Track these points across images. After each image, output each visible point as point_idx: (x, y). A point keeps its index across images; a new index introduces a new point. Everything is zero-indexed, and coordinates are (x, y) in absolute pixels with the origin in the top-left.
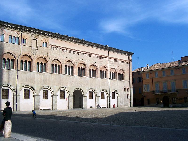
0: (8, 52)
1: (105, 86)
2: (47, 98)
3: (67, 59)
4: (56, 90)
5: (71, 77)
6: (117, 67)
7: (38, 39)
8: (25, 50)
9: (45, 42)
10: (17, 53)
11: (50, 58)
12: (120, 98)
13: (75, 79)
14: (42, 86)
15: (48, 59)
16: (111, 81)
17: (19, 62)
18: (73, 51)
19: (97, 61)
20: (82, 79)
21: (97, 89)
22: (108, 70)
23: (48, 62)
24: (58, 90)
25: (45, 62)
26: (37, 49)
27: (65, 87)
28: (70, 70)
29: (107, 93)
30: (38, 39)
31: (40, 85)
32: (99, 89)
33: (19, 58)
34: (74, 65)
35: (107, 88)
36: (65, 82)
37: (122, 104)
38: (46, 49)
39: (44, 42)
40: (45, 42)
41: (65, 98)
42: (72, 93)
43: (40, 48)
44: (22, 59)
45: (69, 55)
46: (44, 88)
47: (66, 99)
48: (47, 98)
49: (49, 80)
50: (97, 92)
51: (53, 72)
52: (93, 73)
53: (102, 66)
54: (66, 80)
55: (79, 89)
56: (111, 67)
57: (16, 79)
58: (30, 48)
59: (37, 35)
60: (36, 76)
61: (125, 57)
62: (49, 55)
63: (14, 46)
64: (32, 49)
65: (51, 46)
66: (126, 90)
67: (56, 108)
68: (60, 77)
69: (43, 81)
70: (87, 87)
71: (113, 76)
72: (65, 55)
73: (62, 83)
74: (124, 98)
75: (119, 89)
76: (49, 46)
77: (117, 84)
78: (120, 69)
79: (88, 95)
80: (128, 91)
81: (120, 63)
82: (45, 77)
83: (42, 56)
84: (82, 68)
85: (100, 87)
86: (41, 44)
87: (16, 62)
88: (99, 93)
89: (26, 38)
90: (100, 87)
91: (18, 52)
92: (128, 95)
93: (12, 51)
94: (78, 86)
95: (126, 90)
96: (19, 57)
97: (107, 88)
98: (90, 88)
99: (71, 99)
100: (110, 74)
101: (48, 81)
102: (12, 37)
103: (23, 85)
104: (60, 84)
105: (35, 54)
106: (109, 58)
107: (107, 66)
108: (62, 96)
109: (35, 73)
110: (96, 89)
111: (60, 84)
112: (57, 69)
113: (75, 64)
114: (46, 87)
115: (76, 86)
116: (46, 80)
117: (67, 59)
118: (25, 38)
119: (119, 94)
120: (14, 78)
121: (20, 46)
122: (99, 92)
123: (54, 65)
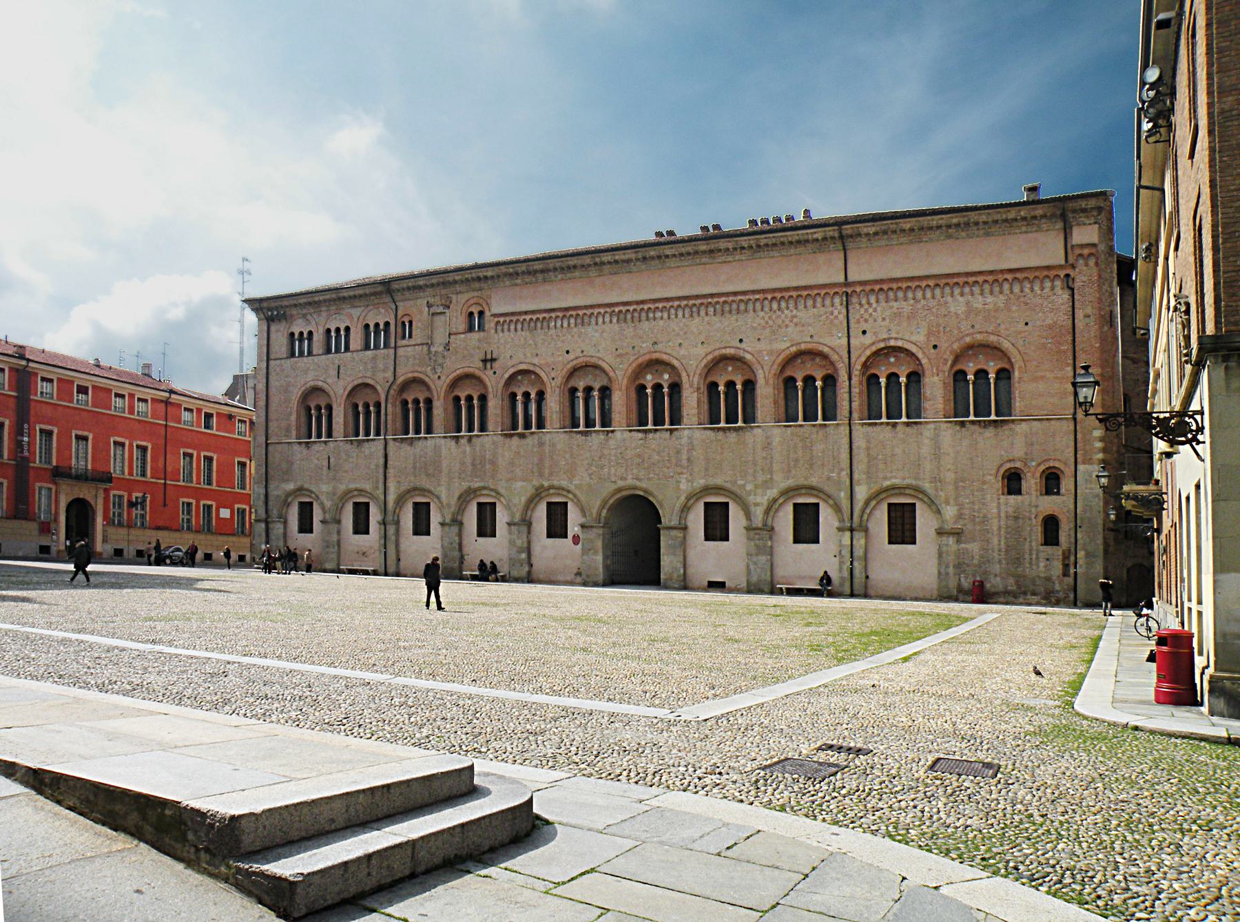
0: (360, 381)
1: (811, 465)
3: (571, 356)
4: (523, 499)
6: (929, 334)
8: (410, 361)
9: (475, 310)
12: (958, 542)
13: (612, 442)
14: (465, 485)
15: (489, 378)
19: (754, 328)
20: (659, 439)
21: (756, 487)
23: (490, 390)
27: (564, 483)
28: (588, 403)
29: (837, 508)
31: (459, 487)
32: (767, 484)
35: (828, 476)
38: (479, 340)
40: (475, 310)
47: (576, 540)
49: (493, 463)
50: (756, 505)
52: (730, 402)
54: (567, 456)
55: (641, 493)
56: (864, 345)
57: (381, 470)
59: (443, 292)
60: (444, 451)
61: (1045, 248)
62: (493, 360)
63: (374, 358)
64: (429, 352)
66: (1031, 483)
68: (541, 444)
69: (470, 468)
70: (683, 481)
73: (547, 471)
74: (997, 542)
75: (950, 476)
76: (490, 324)
77: (926, 450)
81: (957, 304)
82: (478, 449)
83: (467, 370)
85: (778, 477)
95: (1031, 483)
96: (392, 392)
97: (829, 478)
98: (700, 482)
99: (596, 539)
101: (488, 466)
103: (403, 488)
104: (541, 475)
105: (439, 370)
106: (848, 291)
107: (833, 342)
108: (557, 528)
109: (443, 441)
110: (749, 487)
111: (541, 475)
114: (484, 488)
115: (621, 479)
117: (571, 356)
118: (406, 320)
119: (950, 512)
121: (392, 351)
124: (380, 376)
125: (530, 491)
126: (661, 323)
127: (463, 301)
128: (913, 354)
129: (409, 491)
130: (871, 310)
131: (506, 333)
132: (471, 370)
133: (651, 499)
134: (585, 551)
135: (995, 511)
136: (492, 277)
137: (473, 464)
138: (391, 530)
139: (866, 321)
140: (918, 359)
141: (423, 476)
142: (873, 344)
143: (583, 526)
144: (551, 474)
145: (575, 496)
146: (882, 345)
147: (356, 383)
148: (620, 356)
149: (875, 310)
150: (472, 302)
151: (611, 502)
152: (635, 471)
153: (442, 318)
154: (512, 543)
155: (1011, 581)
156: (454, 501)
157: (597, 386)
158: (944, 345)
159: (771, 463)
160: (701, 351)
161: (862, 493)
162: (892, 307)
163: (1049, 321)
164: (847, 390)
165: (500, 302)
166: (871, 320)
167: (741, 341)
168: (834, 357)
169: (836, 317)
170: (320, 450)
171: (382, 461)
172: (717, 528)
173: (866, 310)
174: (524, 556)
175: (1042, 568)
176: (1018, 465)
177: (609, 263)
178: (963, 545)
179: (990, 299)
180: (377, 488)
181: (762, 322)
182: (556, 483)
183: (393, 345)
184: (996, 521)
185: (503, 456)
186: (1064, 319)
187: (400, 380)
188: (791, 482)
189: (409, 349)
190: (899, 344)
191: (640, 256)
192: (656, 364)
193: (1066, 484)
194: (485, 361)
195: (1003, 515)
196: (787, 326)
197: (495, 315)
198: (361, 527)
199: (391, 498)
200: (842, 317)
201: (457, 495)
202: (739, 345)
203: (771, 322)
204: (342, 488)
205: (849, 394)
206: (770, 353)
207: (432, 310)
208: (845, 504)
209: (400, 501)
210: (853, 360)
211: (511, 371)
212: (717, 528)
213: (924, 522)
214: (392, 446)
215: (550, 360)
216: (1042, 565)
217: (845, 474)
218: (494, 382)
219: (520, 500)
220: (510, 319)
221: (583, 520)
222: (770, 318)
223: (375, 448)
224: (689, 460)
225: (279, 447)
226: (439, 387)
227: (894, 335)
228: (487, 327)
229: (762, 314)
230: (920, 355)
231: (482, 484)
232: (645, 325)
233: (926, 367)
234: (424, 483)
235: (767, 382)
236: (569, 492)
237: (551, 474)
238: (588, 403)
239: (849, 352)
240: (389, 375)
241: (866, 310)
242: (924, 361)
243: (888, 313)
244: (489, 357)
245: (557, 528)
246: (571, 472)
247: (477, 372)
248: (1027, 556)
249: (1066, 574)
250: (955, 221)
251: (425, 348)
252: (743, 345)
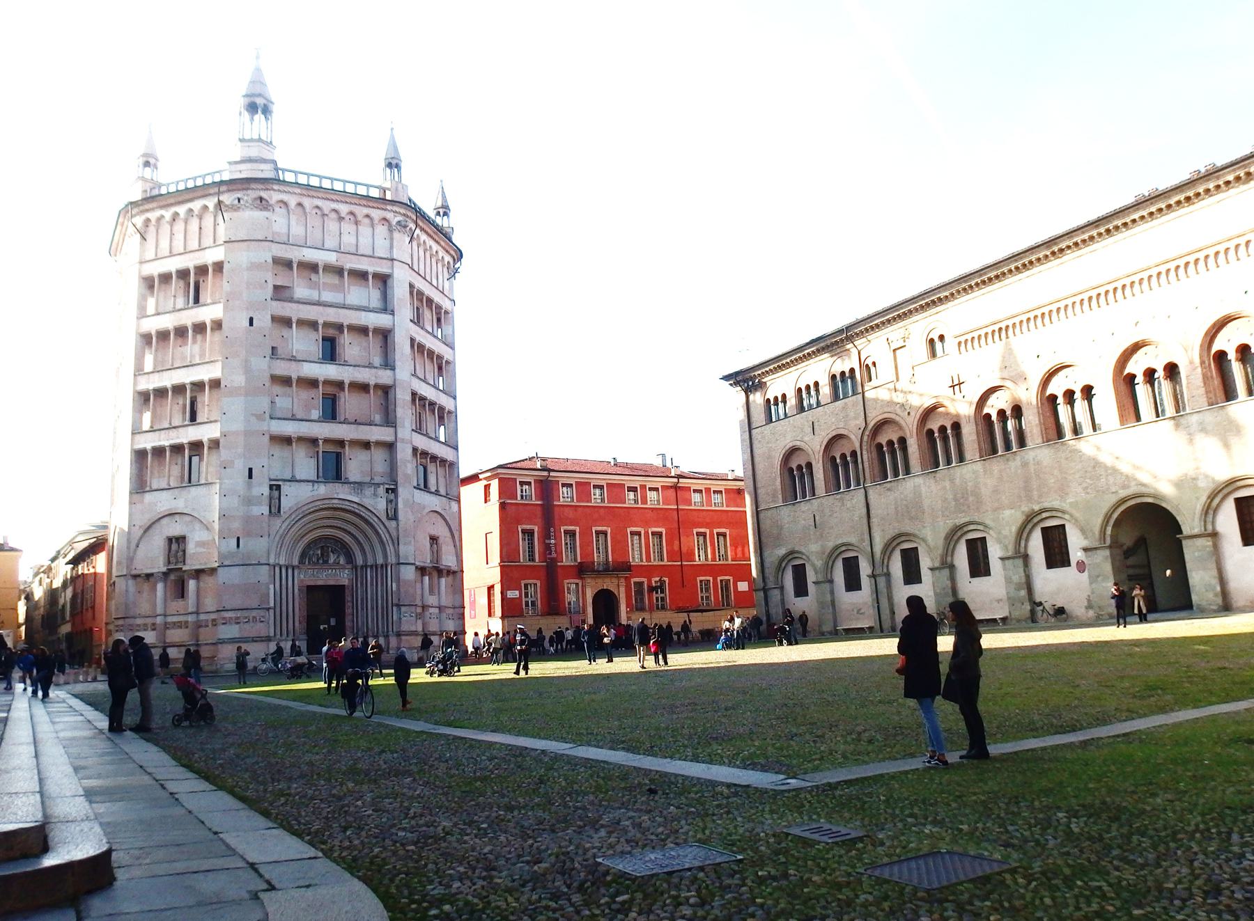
2: (987, 572)
4: (1014, 529)
31: (944, 526)
41: (1073, 561)
46: (965, 529)
47: (1081, 567)
48: (987, 572)
49: (977, 494)
54: (1056, 472)
55: (1150, 500)
57: (865, 521)
60: (923, 490)
68: (1025, 465)
82: (957, 481)
96: (865, 438)
99: (1103, 562)
101: (971, 499)
103: (888, 537)
108: (1057, 554)
115: (1124, 487)
120: (861, 518)
125: (1020, 518)
129: (894, 538)
133: (1164, 505)
134: (1093, 579)
137: (956, 500)
138: (882, 581)
141: (907, 521)
143: (1086, 550)
144: (1040, 496)
145: (1071, 516)
151: (1115, 516)
154: (1008, 580)
156: (941, 542)
165: (953, 318)
170: (805, 510)
171: (864, 510)
174: (1023, 593)
180: (863, 540)
182: (1047, 505)
185: (985, 484)
187: (871, 425)
198: (853, 583)
199: (878, 549)
201: (943, 535)
204: (831, 545)
209: (888, 548)
214: (871, 492)
219: (1011, 530)
221: (1085, 543)
223: (855, 499)
225: (769, 513)
231: (967, 519)
234: (908, 528)
236: (1063, 512)
237: (1040, 496)
245: (1057, 554)
246: (1063, 490)
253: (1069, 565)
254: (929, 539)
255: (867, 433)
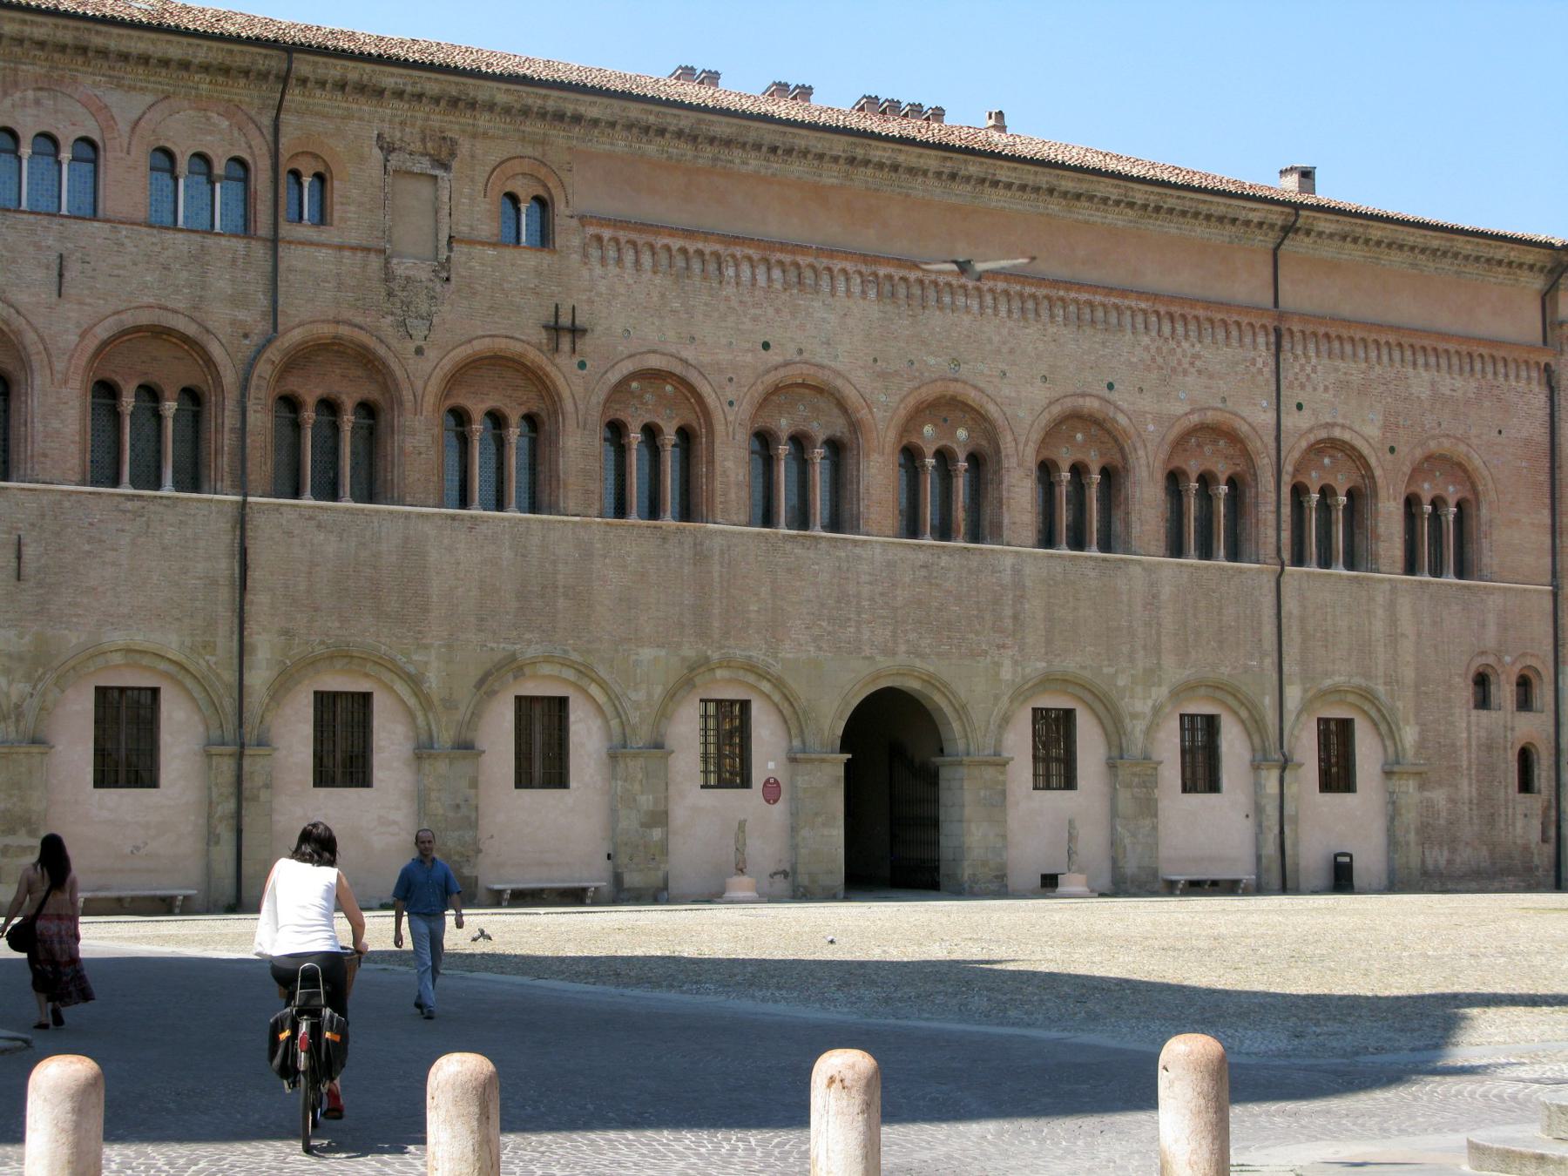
0: (145, 318)
3: (774, 357)
4: (658, 690)
5: (820, 553)
6: (1385, 427)
7: (446, 167)
8: (322, 285)
9: (525, 190)
10: (233, 323)
11: (582, 365)
12: (1422, 787)
15: (563, 371)
16: (1317, 588)
17: (261, 419)
18: (844, 271)
22: (1265, 464)
23: (568, 405)
24: (673, 696)
25: (534, 406)
26: (444, 272)
27: (758, 655)
29: (1253, 726)
30: (455, 164)
32: (1151, 676)
33: (254, 381)
34: (855, 426)
36: (754, 608)
37: (1453, 851)
39: (513, 198)
42: (832, 718)
43: (472, 264)
44: (293, 385)
45: (793, 314)
47: (772, 791)
48: (557, 777)
50: (1134, 716)
51: (621, 510)
52: (1082, 506)
53: (1195, 419)
54: (765, 591)
57: (225, 594)
58: (365, 266)
62: (576, 331)
64: (388, 277)
65: (591, 230)
66: (1504, 692)
67: (655, 878)
68: (701, 557)
71: (1330, 524)
72: (755, 319)
76: (568, 235)
78: (1419, 453)
79: (1019, 742)
80: (1525, 702)
81: (1420, 381)
83: (501, 344)
84: (944, 457)
85: (1169, 661)
86: (477, 212)
87: (230, 420)
88: (1150, 731)
89: (321, 169)
90: (1169, 661)
91: (241, 315)
92: (1526, 758)
93: (181, 306)
94: (903, 648)
95: (1504, 692)
100: (1286, 510)
101: (562, 603)
102: (183, 165)
107: (1256, 415)
112: (659, 465)
113: (864, 413)
116: (544, 587)
118: (307, 168)
119: (1409, 735)
121: (260, 251)
122: (1157, 710)
123: (635, 437)
124: (220, 317)
126: (966, 319)
127: (493, 159)
128: (1361, 456)
130: (1308, 369)
131: (613, 269)
132: (517, 347)
135: (1464, 735)
136: (595, 122)
139: (1302, 387)
140: (1368, 467)
142: (1311, 430)
146: (1323, 434)
147: (129, 320)
148: (883, 375)
149: (1314, 370)
150: (517, 166)
152: (912, 636)
153: (425, 189)
155: (1485, 852)
157: (820, 433)
158: (1403, 450)
159: (1159, 634)
160: (1038, 394)
161: (1293, 694)
162: (1336, 370)
163: (1524, 434)
164: (1272, 507)
166: (1309, 389)
167: (1110, 386)
168: (1254, 445)
169: (1260, 371)
171: (225, 567)
172: (1055, 757)
173: (1302, 369)
175: (1519, 831)
176: (1491, 660)
177: (880, 166)
178: (1427, 794)
179: (1459, 383)
180: (209, 646)
181: (1146, 356)
183: (264, 229)
184: (1465, 752)
186: (1540, 433)
188: (1187, 674)
189: (322, 254)
190: (1347, 436)
191: (948, 167)
192: (947, 407)
193: (1543, 694)
194: (554, 329)
195: (1474, 743)
196: (1185, 373)
197: (584, 220)
200: (1268, 372)
202: (1106, 393)
203: (1160, 360)
205: (1269, 518)
206: (1158, 419)
207: (395, 160)
208: (1271, 717)
210: (1283, 454)
211: (628, 367)
212: (1055, 757)
213: (1367, 753)
215: (724, 357)
216: (1519, 825)
217: (1269, 662)
218: (581, 392)
220: (631, 236)
222: (1159, 349)
224: (1015, 617)
226: (422, 377)
227: (1340, 421)
228: (559, 241)
229: (1146, 340)
230: (1373, 461)
232: (936, 320)
233: (1381, 482)
235: (1151, 475)
236: (763, 675)
238: (805, 469)
239: (1278, 439)
240: (253, 317)
241: (1302, 369)
242: (1378, 473)
243: (1332, 378)
244: (565, 320)
245: (730, 762)
247: (534, 356)
248: (1503, 811)
249: (1545, 840)
250: (1435, 244)
251: (375, 262)
252: (1114, 396)
253: (746, 783)
254: (434, 682)
255: (274, 354)
